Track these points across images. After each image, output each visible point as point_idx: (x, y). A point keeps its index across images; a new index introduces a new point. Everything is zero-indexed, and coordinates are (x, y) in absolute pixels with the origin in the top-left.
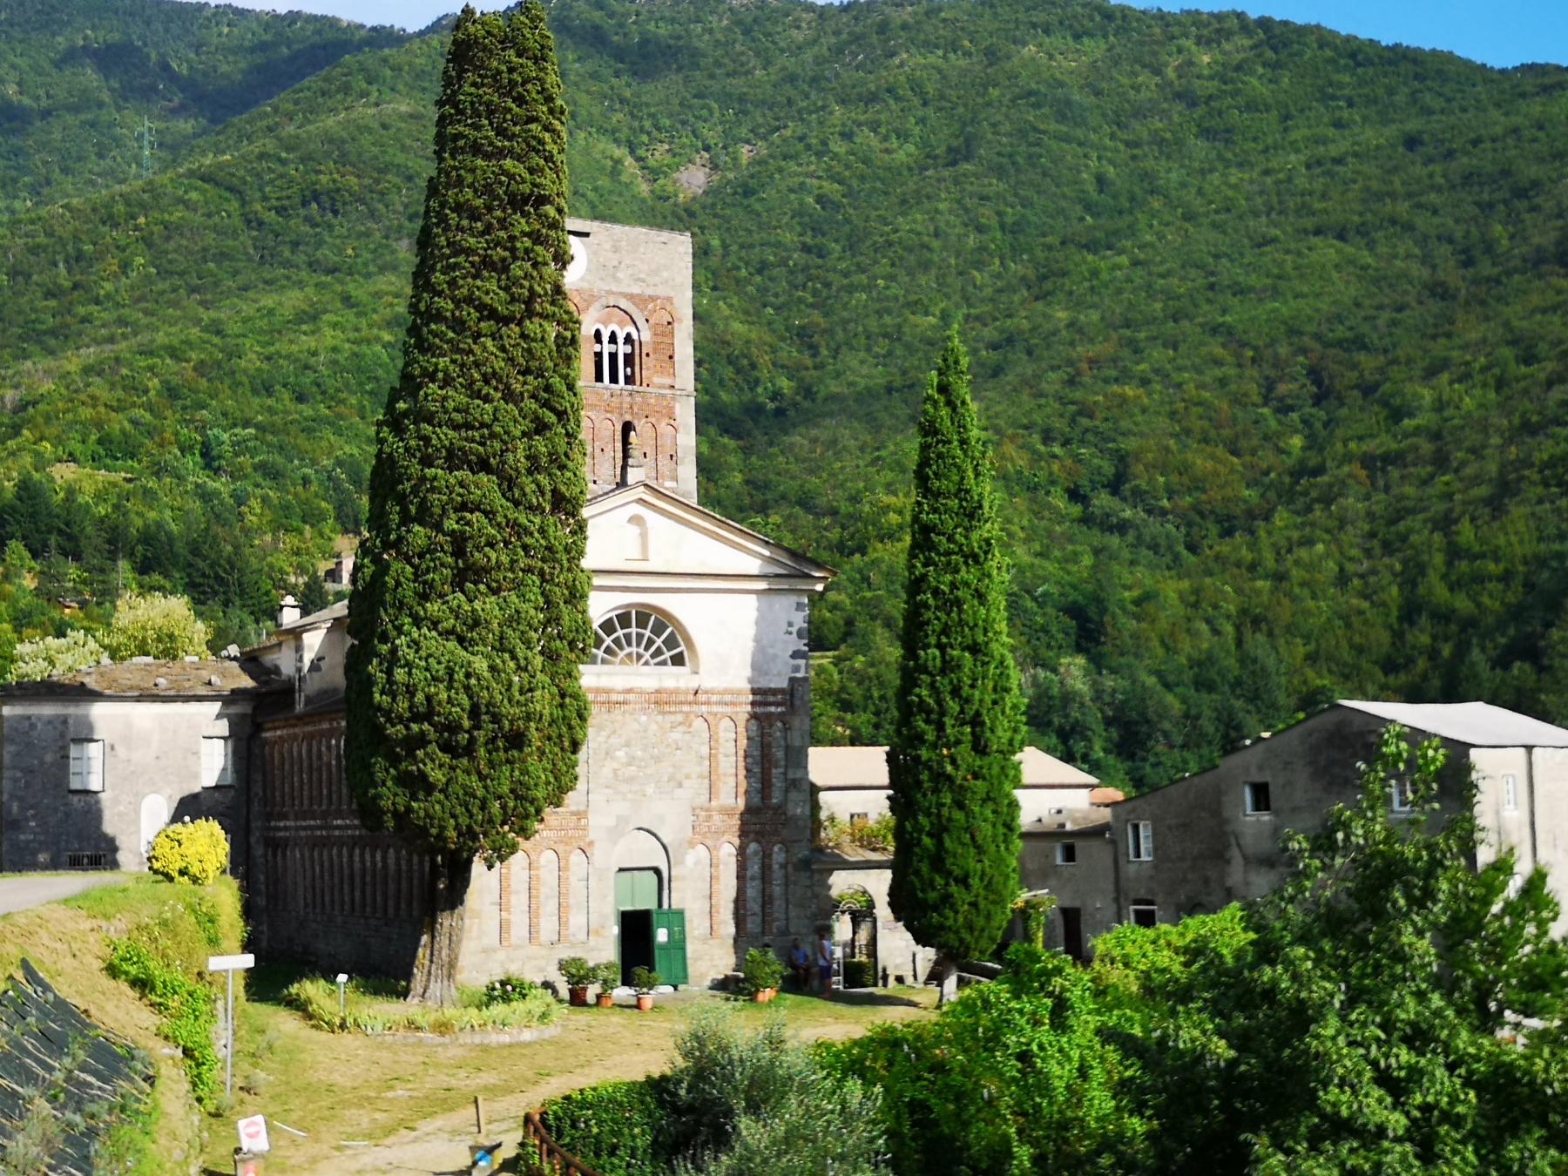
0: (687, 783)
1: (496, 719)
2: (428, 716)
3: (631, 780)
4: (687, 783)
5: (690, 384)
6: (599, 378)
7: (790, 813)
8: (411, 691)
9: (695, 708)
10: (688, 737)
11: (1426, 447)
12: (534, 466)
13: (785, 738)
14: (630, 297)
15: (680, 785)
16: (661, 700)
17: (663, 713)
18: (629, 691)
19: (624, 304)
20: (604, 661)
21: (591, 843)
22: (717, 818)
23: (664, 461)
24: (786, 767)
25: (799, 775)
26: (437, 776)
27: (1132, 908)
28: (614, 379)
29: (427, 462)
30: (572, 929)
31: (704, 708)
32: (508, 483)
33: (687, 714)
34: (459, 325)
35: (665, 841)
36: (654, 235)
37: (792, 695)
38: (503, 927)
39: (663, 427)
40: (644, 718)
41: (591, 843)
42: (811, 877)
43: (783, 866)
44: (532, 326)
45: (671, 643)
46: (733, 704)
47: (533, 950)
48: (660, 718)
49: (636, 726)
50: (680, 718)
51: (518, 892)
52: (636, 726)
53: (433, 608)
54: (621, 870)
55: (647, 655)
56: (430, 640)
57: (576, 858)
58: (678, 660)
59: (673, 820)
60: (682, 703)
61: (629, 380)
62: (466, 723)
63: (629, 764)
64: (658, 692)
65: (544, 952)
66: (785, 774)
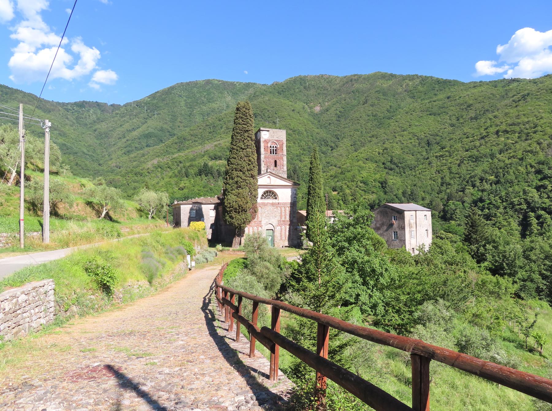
1: (242, 208)
2: (232, 207)
3: (268, 216)
5: (286, 154)
6: (271, 153)
8: (230, 204)
11: (447, 154)
12: (248, 170)
14: (276, 140)
16: (273, 204)
19: (275, 141)
23: (281, 166)
26: (234, 216)
28: (273, 153)
29: (233, 170)
32: (244, 173)
34: (237, 150)
36: (279, 130)
39: (281, 161)
43: (292, 229)
44: (248, 150)
45: (275, 196)
53: (233, 192)
56: (233, 196)
57: (260, 228)
58: (276, 198)
59: (275, 222)
61: (276, 153)
62: (238, 208)
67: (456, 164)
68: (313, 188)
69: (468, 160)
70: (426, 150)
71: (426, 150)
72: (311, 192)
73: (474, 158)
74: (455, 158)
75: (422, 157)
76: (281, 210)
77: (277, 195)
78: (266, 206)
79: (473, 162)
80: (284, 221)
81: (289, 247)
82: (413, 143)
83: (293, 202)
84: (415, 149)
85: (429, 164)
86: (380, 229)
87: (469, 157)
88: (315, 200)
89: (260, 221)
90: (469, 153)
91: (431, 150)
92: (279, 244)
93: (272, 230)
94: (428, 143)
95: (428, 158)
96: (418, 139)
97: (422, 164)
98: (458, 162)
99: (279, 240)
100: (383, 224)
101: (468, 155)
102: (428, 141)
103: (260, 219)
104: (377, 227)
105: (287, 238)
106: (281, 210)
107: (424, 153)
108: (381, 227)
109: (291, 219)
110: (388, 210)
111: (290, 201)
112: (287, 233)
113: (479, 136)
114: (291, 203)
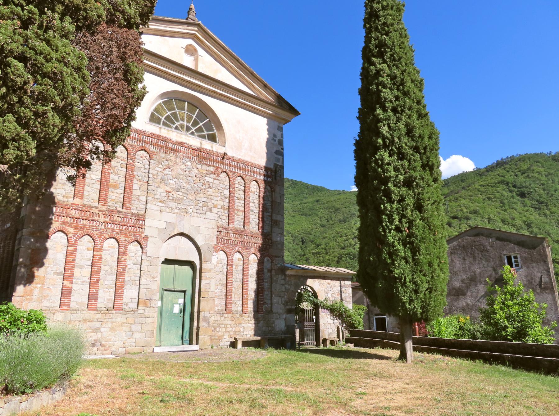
0: (214, 210)
4: (214, 210)
7: (274, 240)
9: (221, 166)
10: (216, 182)
11: (323, 251)
13: (272, 197)
15: (211, 211)
17: (203, 164)
18: (181, 144)
20: (164, 124)
21: (146, 238)
22: (232, 237)
24: (272, 213)
25: (278, 218)
27: (374, 317)
30: (125, 300)
31: (227, 168)
33: (217, 167)
35: (200, 244)
37: (276, 172)
38: (66, 293)
40: (189, 163)
41: (146, 238)
42: (284, 279)
43: (270, 271)
46: (244, 170)
47: (91, 314)
48: (199, 166)
49: (183, 167)
50: (212, 169)
51: (82, 267)
52: (183, 167)
54: (167, 262)
55: (193, 129)
57: (134, 248)
58: (212, 138)
60: (213, 161)
63: (177, 190)
64: (199, 149)
65: (99, 316)
66: (271, 216)
67: (334, 260)
68: (393, 77)
69: (346, 257)
70: (301, 247)
71: (301, 247)
72: (387, 94)
73: (351, 255)
74: (332, 255)
75: (297, 254)
76: (231, 188)
77: (219, 126)
78: (171, 156)
79: (351, 259)
80: (239, 233)
81: (256, 344)
82: (288, 240)
83: (272, 166)
84: (291, 246)
85: (306, 261)
86: (464, 294)
87: (347, 254)
88: (407, 125)
89: (140, 218)
90: (346, 251)
91: (306, 247)
92: (220, 331)
93: (190, 264)
94: (303, 241)
95: (304, 255)
96: (292, 236)
97: (299, 260)
98: (336, 259)
99: (218, 313)
100: (473, 280)
101: (346, 253)
102: (302, 238)
103: (137, 207)
104: (454, 289)
105: (250, 306)
106: (231, 188)
107: (300, 251)
108: (468, 287)
109: (267, 228)
110: (487, 242)
111: (262, 161)
112: (252, 285)
113: (352, 236)
114: (266, 169)
